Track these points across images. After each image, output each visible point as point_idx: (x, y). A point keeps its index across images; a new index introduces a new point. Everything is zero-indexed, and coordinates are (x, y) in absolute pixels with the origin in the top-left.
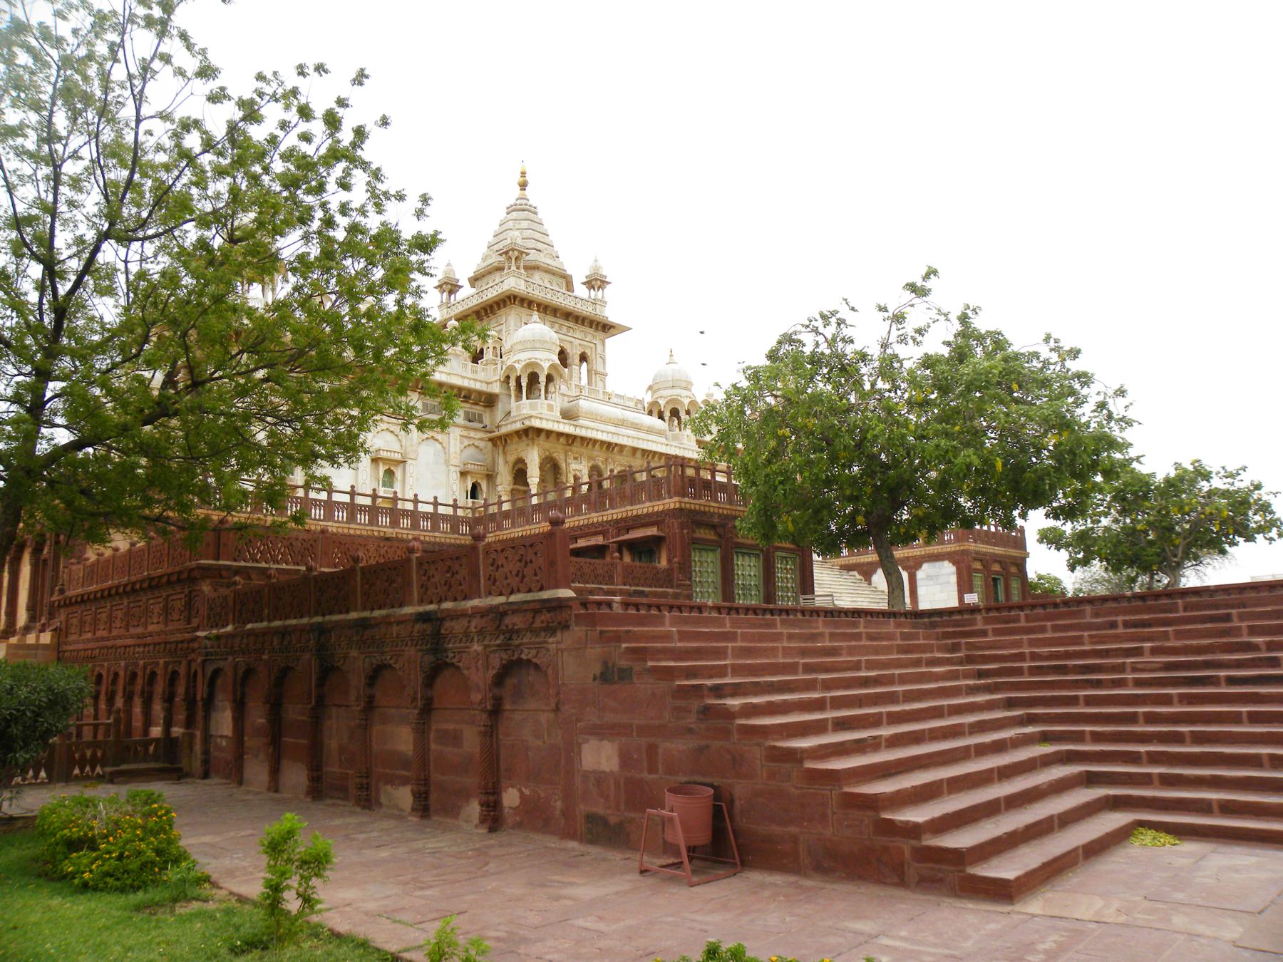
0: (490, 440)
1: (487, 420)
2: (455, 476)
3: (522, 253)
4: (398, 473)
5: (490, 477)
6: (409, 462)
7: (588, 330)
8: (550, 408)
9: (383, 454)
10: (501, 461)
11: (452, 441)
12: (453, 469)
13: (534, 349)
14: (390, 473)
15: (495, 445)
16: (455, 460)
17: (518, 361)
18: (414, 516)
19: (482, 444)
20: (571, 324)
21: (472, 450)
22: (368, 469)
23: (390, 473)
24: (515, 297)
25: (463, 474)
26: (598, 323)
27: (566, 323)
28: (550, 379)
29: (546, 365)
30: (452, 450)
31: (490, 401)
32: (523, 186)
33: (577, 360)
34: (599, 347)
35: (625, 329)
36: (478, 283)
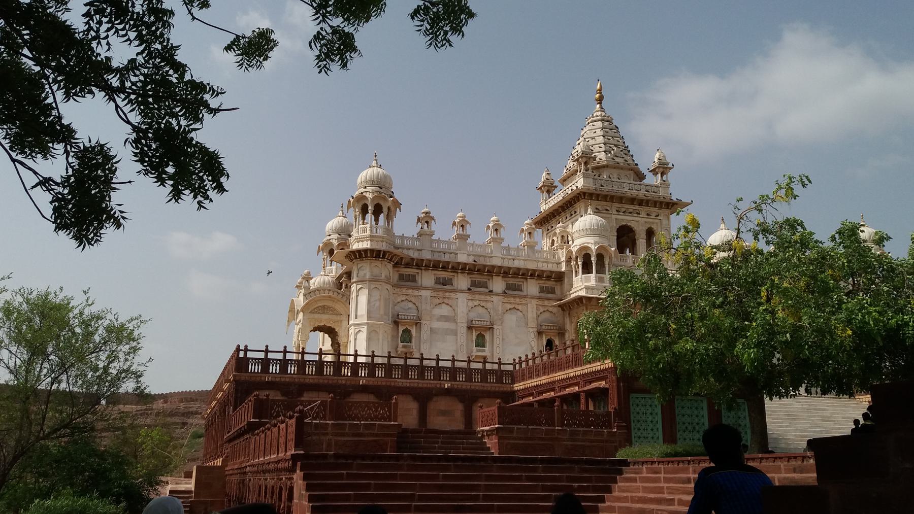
0: (560, 306)
1: (558, 291)
2: (532, 335)
3: (590, 158)
4: (487, 337)
5: (562, 334)
6: (495, 327)
7: (652, 209)
8: (600, 280)
9: (475, 323)
10: (567, 321)
11: (530, 310)
12: (531, 330)
13: (587, 235)
14: (481, 337)
15: (563, 310)
16: (533, 324)
17: (576, 244)
18: (438, 370)
19: (555, 310)
20: (637, 207)
21: (547, 315)
22: (465, 335)
23: (481, 337)
24: (584, 193)
25: (540, 333)
26: (661, 203)
27: (632, 207)
28: (600, 257)
29: (594, 248)
30: (530, 315)
31: (559, 277)
32: (600, 100)
33: (644, 235)
34: (665, 222)
35: (687, 204)
36: (566, 183)
